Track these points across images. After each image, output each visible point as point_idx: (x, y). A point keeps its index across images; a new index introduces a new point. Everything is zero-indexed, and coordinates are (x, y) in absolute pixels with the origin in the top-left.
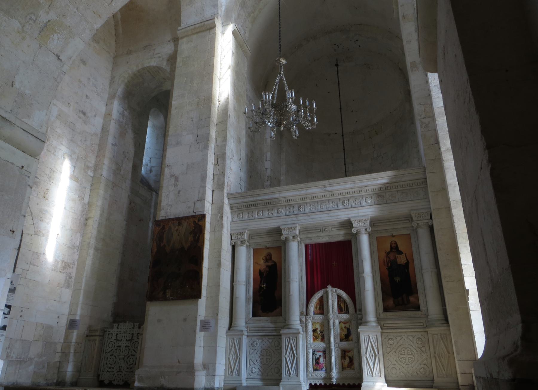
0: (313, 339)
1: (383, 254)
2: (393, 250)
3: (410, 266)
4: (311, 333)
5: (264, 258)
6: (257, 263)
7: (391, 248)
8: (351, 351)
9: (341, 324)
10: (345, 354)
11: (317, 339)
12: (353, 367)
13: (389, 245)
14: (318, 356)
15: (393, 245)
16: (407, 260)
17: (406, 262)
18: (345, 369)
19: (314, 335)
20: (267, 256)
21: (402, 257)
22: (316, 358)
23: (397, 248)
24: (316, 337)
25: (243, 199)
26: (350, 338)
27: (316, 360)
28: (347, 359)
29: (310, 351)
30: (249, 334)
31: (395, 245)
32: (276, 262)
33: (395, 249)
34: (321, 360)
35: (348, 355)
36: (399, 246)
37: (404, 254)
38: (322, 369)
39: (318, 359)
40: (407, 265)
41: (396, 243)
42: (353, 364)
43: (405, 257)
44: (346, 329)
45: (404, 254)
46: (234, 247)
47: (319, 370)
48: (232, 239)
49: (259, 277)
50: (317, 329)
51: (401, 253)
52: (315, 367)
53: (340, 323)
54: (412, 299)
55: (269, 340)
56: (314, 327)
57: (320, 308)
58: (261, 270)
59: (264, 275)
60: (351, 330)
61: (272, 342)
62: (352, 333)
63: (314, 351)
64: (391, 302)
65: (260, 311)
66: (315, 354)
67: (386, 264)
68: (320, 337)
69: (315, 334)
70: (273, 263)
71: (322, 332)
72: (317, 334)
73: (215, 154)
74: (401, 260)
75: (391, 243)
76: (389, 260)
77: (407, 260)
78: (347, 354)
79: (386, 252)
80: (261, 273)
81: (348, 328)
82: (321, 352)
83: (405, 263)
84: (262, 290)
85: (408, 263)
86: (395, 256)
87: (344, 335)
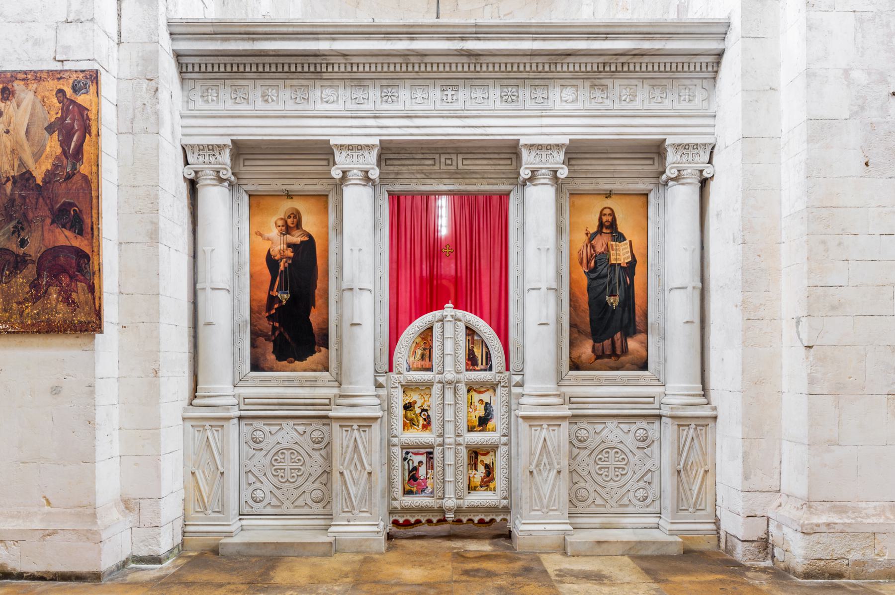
0: (405, 425)
1: (582, 239)
2: (604, 230)
3: (638, 269)
4: (399, 411)
5: (280, 223)
6: (261, 235)
7: (601, 225)
8: (491, 453)
9: (471, 393)
10: (476, 458)
11: (414, 425)
12: (492, 485)
13: (598, 216)
14: (416, 464)
15: (605, 219)
16: (633, 256)
17: (630, 259)
18: (475, 490)
19: (406, 417)
20: (289, 217)
21: (621, 248)
22: (411, 468)
23: (613, 225)
24: (411, 420)
26: (490, 425)
27: (410, 472)
28: (481, 469)
29: (398, 452)
30: (244, 413)
31: (610, 218)
32: (314, 236)
34: (422, 471)
35: (482, 461)
36: (618, 222)
37: (627, 241)
38: (423, 491)
39: (415, 469)
41: (612, 214)
42: (493, 479)
43: (629, 249)
44: (483, 405)
45: (627, 241)
46: (193, 185)
47: (416, 494)
48: (187, 163)
49: (267, 271)
50: (415, 402)
51: (620, 238)
52: (408, 488)
53: (469, 391)
54: (633, 344)
55: (296, 427)
56: (407, 398)
57: (423, 357)
58: (272, 253)
59: (282, 268)
60: (494, 408)
61: (305, 432)
62: (494, 413)
63: (407, 453)
64: (586, 349)
65: (272, 357)
66: (409, 458)
67: (585, 261)
68: (421, 422)
69: (410, 414)
70: (306, 239)
71: (426, 410)
72: (415, 414)
74: (621, 255)
76: (592, 252)
77: (633, 256)
78: (480, 458)
79: (587, 234)
80: (272, 262)
81: (487, 403)
82: (422, 454)
83: (627, 263)
84: (276, 306)
85: (633, 263)
87: (477, 417)
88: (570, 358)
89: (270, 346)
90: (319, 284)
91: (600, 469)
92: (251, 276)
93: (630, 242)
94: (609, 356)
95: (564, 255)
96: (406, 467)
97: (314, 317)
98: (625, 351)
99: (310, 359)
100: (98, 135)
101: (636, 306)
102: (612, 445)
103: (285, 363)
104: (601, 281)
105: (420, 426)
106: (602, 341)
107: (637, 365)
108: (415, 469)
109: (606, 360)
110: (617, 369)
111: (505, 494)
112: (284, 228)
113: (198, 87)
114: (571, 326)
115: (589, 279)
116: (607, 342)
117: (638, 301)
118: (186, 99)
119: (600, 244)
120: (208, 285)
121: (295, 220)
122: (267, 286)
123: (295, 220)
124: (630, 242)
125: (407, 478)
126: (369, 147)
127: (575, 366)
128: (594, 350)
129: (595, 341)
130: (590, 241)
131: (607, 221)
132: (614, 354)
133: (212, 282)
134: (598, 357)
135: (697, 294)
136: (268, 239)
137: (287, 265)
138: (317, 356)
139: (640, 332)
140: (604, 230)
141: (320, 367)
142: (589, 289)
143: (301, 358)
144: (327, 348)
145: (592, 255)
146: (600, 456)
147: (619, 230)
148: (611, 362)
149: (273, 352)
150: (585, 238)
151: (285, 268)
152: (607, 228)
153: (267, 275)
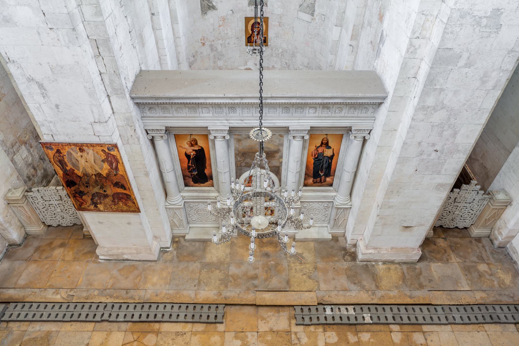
1: (313, 148)
2: (323, 145)
7: (322, 143)
13: (321, 141)
15: (324, 142)
17: (332, 154)
20: (192, 141)
25: (154, 100)
31: (326, 141)
33: (326, 144)
36: (329, 143)
37: (332, 149)
40: (332, 157)
46: (152, 141)
48: (148, 134)
49: (186, 158)
54: (328, 179)
59: (192, 157)
64: (311, 181)
65: (192, 183)
67: (314, 155)
73: (90, 38)
79: (316, 147)
85: (334, 155)
86: (323, 150)
89: (191, 180)
90: (207, 162)
92: (180, 160)
93: (333, 149)
94: (319, 183)
95: (305, 155)
97: (206, 171)
98: (325, 181)
99: (206, 183)
100: (123, 163)
101: (332, 169)
103: (197, 184)
104: (320, 161)
106: (317, 178)
107: (328, 185)
109: (317, 184)
110: (321, 186)
112: (190, 145)
113: (146, 108)
115: (314, 160)
117: (333, 167)
118: (142, 112)
119: (320, 150)
120: (166, 171)
121: (195, 142)
122: (187, 163)
123: (195, 142)
124: (333, 149)
126: (225, 130)
127: (305, 185)
128: (313, 181)
129: (314, 178)
130: (317, 149)
131: (325, 142)
132: (321, 181)
133: (167, 170)
134: (314, 183)
135: (353, 174)
136: (185, 148)
137: (193, 156)
138: (209, 182)
139: (332, 176)
141: (210, 186)
142: (314, 164)
143: (203, 182)
144: (213, 180)
147: (329, 145)
148: (319, 184)
149: (192, 181)
150: (315, 148)
151: (193, 157)
152: (324, 144)
153: (186, 159)
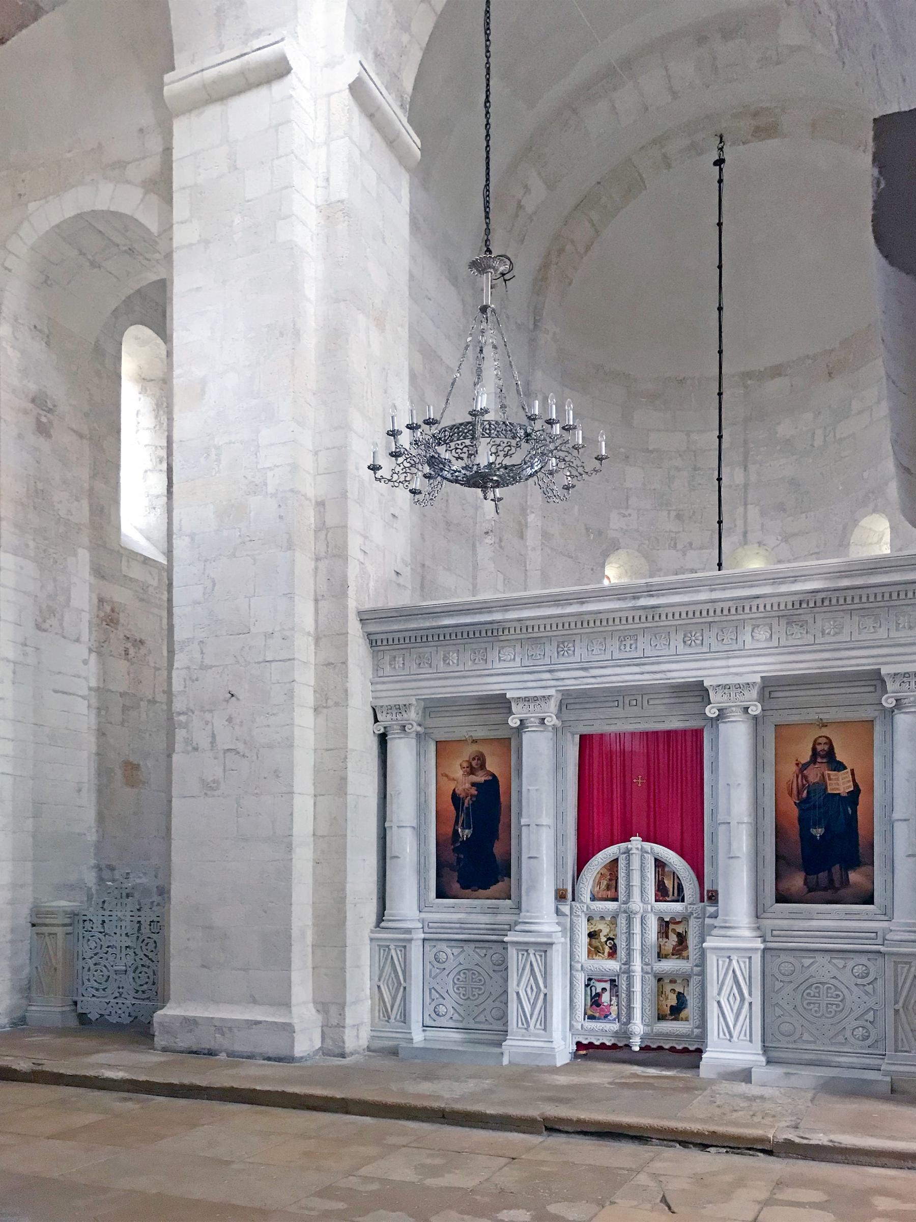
2: (819, 760)
13: (811, 746)
15: (819, 748)
19: (590, 944)
23: (830, 754)
24: (596, 948)
31: (826, 748)
34: (605, 998)
38: (606, 1017)
39: (598, 995)
41: (830, 743)
50: (601, 931)
52: (589, 1012)
63: (590, 980)
64: (797, 881)
68: (607, 950)
71: (613, 939)
72: (600, 942)
74: (840, 784)
75: (815, 741)
79: (797, 764)
82: (606, 981)
88: (776, 889)
91: (809, 1004)
94: (825, 889)
96: (589, 993)
102: (824, 980)
105: (606, 954)
106: (817, 873)
108: (598, 995)
109: (820, 893)
111: (697, 1023)
114: (778, 857)
116: (823, 875)
119: (813, 775)
125: (589, 1003)
127: (781, 898)
128: (806, 883)
140: (819, 760)
142: (801, 820)
145: (803, 785)
146: (808, 991)
150: (794, 768)
152: (822, 757)
